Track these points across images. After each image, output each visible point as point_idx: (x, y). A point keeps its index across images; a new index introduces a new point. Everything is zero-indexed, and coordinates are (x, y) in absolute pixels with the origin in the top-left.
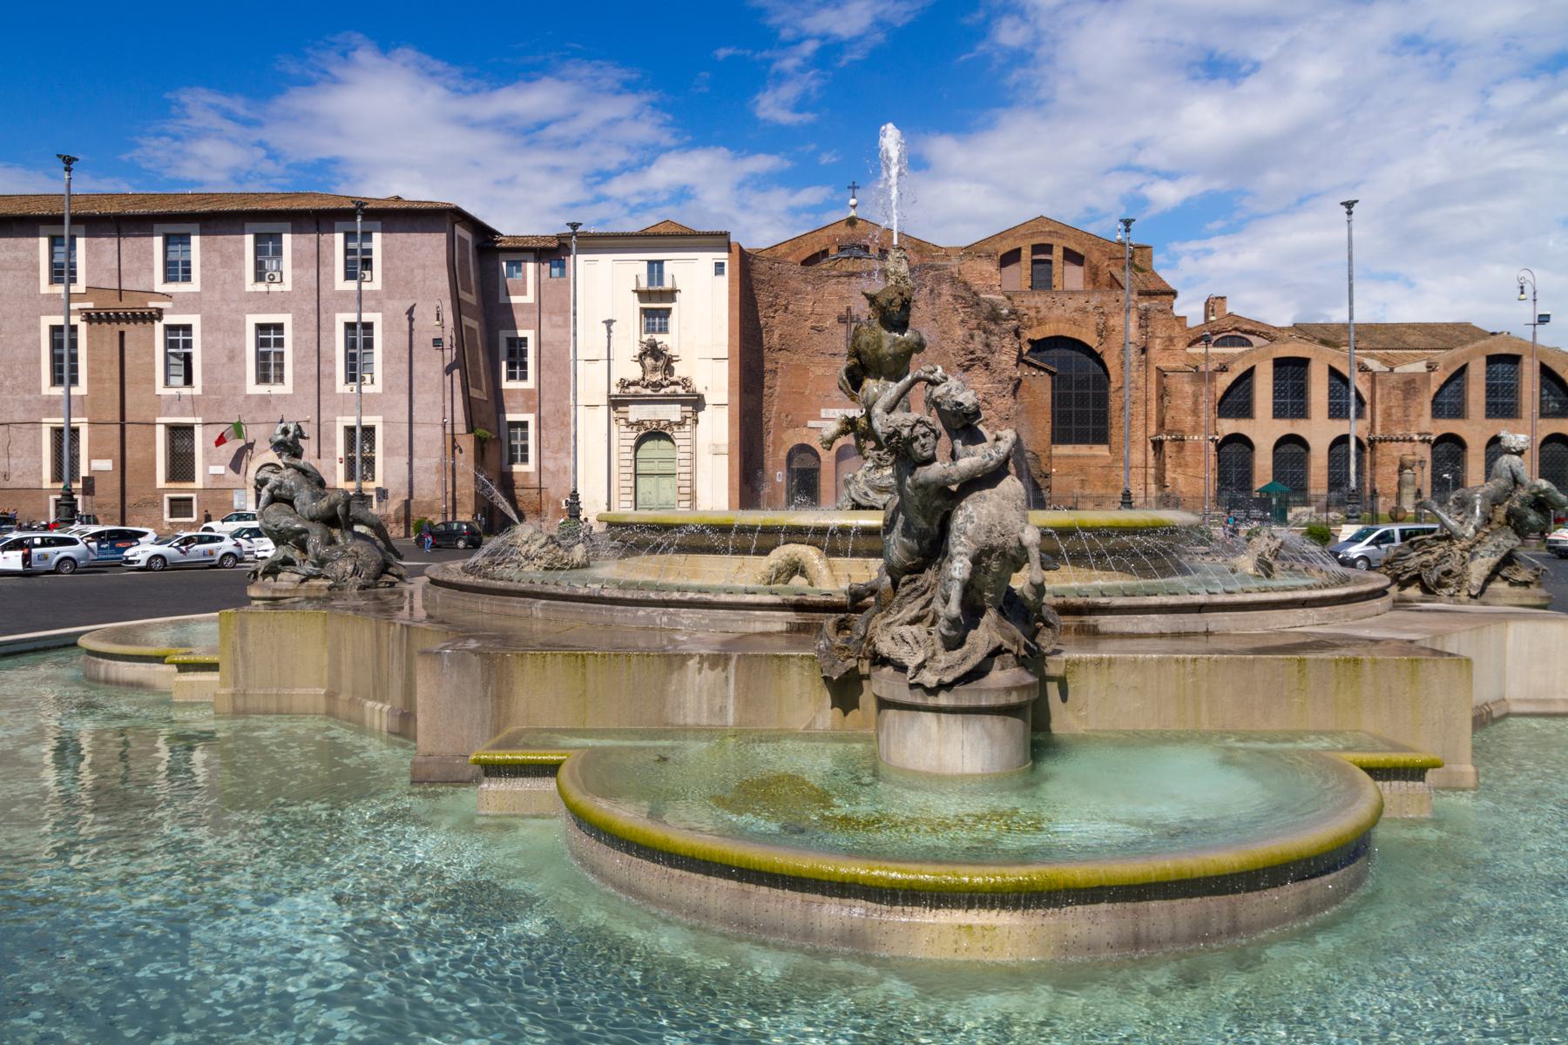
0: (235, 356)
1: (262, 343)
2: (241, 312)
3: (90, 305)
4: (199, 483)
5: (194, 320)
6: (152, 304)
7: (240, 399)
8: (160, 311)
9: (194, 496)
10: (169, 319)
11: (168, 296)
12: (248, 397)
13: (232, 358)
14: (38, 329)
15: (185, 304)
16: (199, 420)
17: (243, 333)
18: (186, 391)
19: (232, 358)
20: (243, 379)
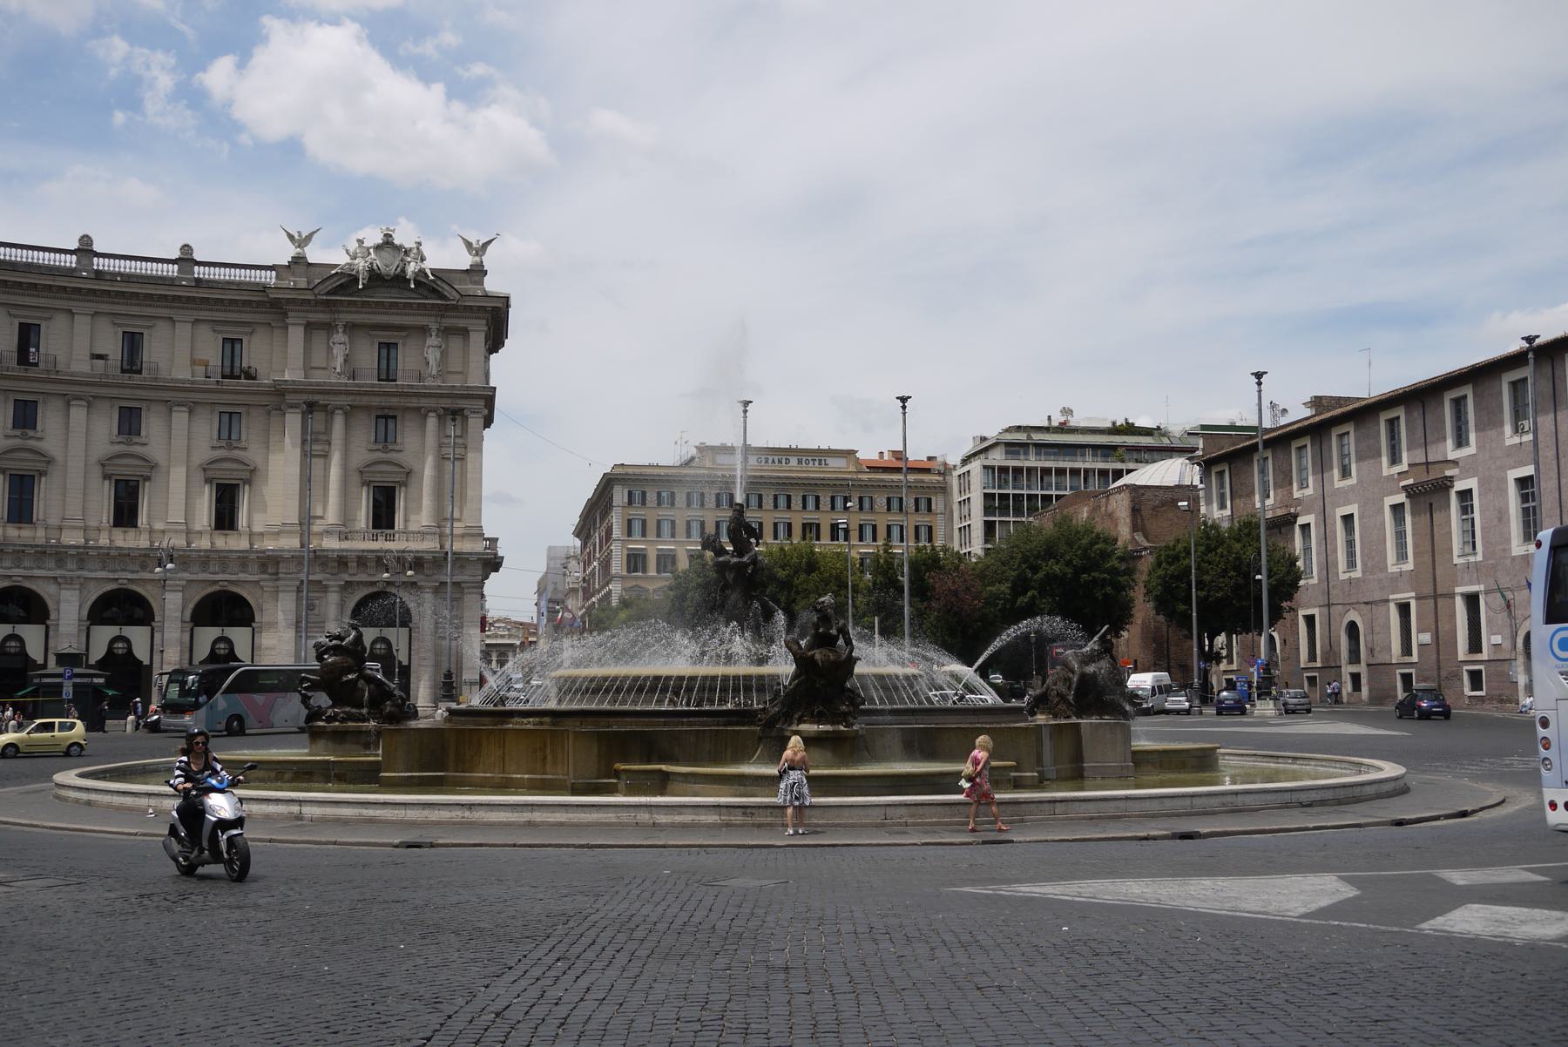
0: (1502, 515)
1: (1525, 498)
2: (1504, 469)
3: (1411, 481)
4: (1484, 656)
5: (1471, 483)
6: (1448, 473)
7: (1508, 561)
8: (1451, 479)
9: (1481, 667)
10: (1460, 485)
11: (1455, 463)
12: (1514, 558)
13: (1500, 519)
14: (1381, 510)
15: (1469, 468)
16: (1482, 588)
17: (1506, 490)
18: (1472, 559)
19: (1500, 519)
20: (1508, 540)
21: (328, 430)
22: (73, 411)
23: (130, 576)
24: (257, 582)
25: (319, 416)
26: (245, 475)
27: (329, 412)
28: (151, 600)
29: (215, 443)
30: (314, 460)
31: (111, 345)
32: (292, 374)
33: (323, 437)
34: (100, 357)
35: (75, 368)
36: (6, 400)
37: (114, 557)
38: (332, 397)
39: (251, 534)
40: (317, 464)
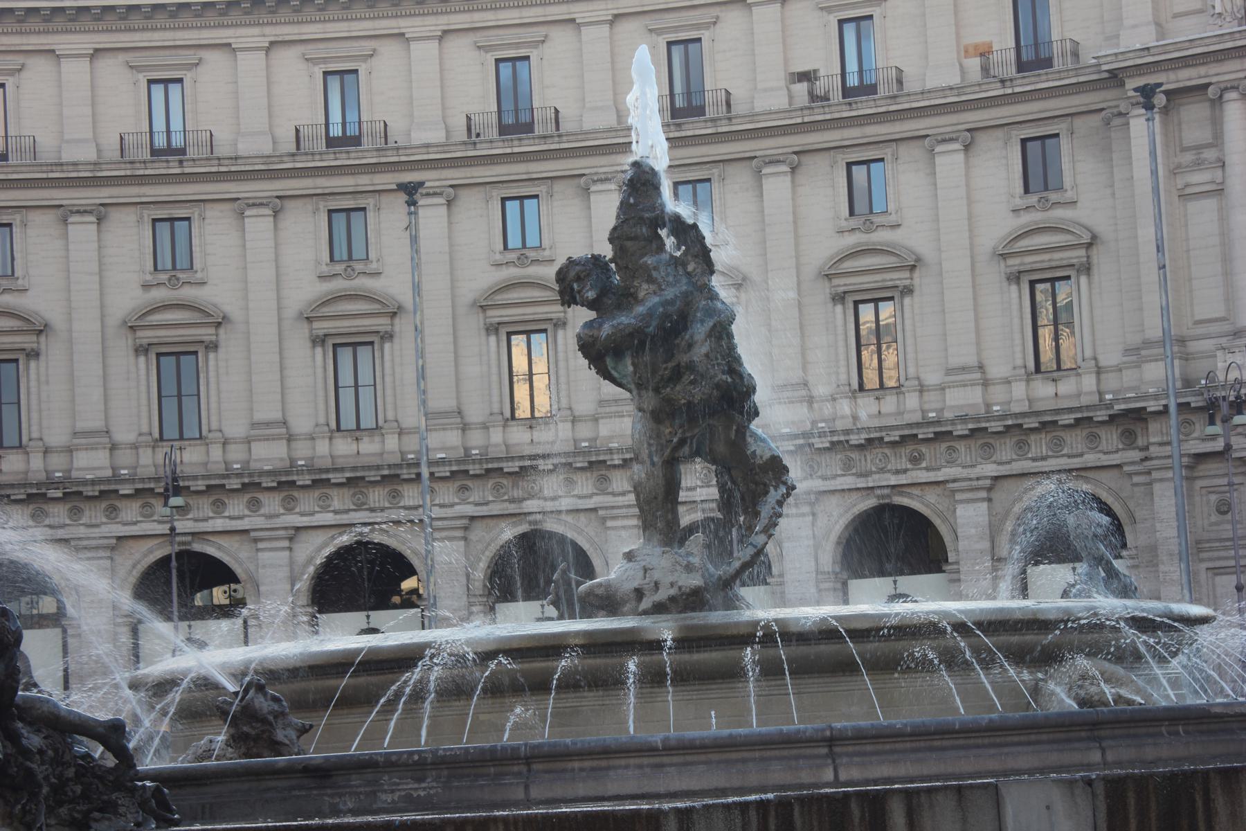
21: (1218, 140)
22: (769, 185)
23: (894, 480)
24: (1119, 466)
25: (1193, 114)
26: (1077, 255)
27: (1218, 102)
28: (937, 522)
29: (1019, 202)
30: (1194, 206)
31: (817, 52)
32: (1137, 37)
33: (1210, 154)
34: (806, 76)
35: (761, 105)
36: (316, 211)
37: (860, 447)
38: (1214, 69)
39: (1099, 371)
40: (1203, 214)
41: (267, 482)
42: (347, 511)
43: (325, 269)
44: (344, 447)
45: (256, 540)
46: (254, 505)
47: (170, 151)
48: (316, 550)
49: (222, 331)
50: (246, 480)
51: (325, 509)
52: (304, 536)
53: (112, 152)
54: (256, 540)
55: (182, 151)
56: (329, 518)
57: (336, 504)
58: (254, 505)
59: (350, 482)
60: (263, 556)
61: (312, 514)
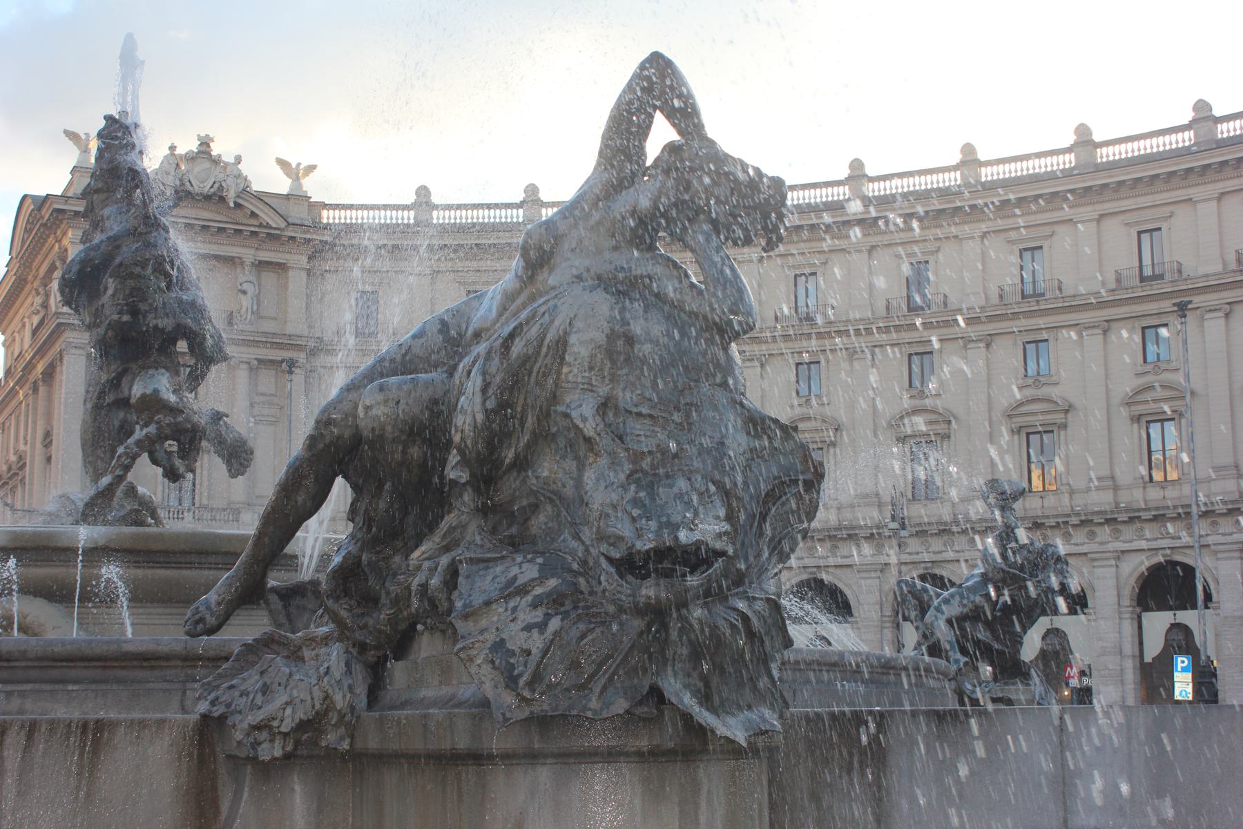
41: (1097, 519)
42: (1156, 539)
43: (1140, 369)
44: (1154, 494)
45: (1094, 560)
46: (1092, 535)
47: (1035, 295)
48: (1137, 565)
49: (1069, 415)
50: (1083, 518)
51: (1141, 538)
52: (1127, 557)
53: (995, 300)
54: (1094, 560)
55: (1043, 295)
56: (1144, 544)
57: (1148, 535)
58: (1092, 535)
59: (1155, 518)
60: (1098, 571)
61: (1131, 541)
